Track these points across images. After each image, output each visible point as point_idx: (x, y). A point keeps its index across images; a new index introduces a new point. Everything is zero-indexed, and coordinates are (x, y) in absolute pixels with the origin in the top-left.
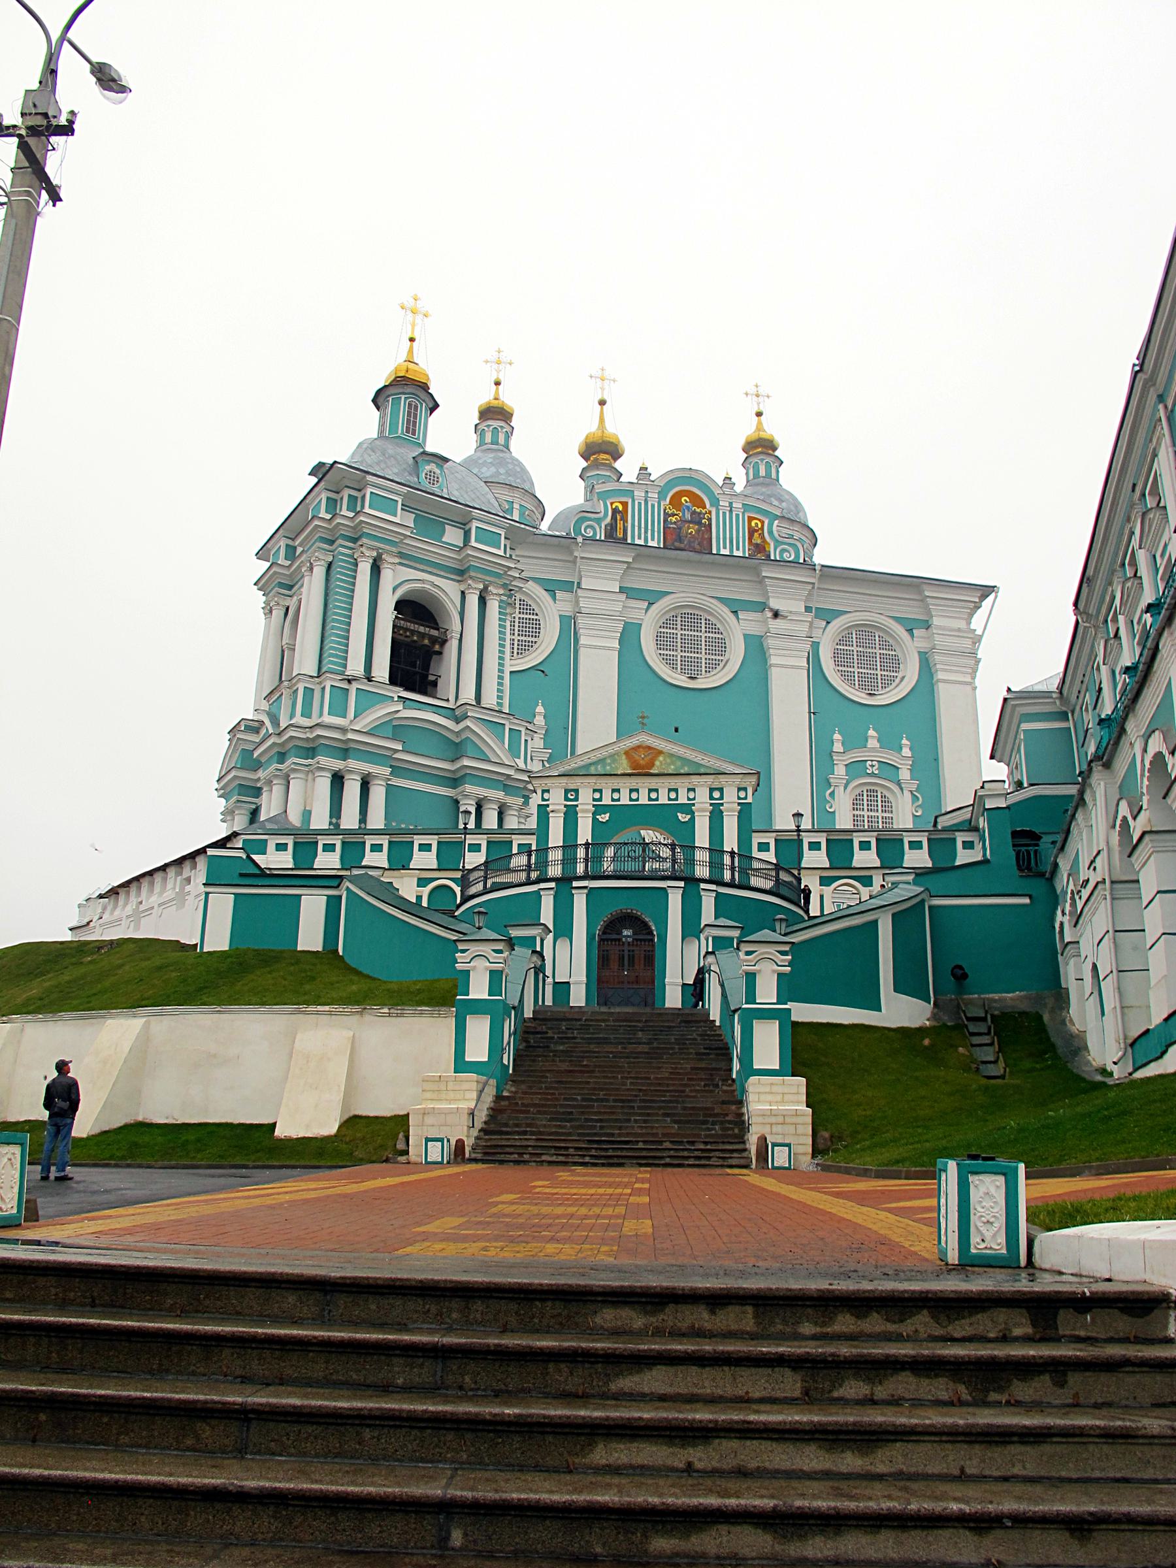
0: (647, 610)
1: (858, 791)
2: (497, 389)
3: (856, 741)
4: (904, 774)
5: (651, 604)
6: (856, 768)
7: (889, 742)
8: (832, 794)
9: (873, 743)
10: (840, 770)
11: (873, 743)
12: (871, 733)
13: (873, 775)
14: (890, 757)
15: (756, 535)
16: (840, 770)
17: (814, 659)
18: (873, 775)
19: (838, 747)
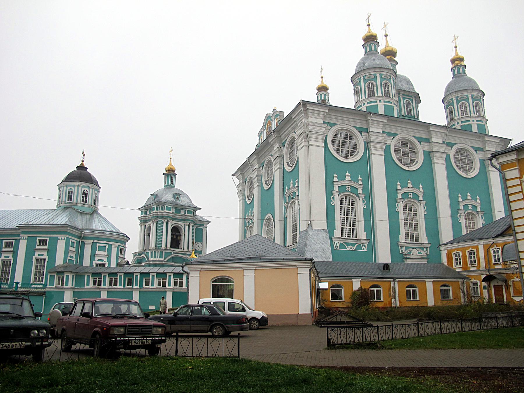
0: (263, 168)
2: (322, 80)
13: (292, 198)
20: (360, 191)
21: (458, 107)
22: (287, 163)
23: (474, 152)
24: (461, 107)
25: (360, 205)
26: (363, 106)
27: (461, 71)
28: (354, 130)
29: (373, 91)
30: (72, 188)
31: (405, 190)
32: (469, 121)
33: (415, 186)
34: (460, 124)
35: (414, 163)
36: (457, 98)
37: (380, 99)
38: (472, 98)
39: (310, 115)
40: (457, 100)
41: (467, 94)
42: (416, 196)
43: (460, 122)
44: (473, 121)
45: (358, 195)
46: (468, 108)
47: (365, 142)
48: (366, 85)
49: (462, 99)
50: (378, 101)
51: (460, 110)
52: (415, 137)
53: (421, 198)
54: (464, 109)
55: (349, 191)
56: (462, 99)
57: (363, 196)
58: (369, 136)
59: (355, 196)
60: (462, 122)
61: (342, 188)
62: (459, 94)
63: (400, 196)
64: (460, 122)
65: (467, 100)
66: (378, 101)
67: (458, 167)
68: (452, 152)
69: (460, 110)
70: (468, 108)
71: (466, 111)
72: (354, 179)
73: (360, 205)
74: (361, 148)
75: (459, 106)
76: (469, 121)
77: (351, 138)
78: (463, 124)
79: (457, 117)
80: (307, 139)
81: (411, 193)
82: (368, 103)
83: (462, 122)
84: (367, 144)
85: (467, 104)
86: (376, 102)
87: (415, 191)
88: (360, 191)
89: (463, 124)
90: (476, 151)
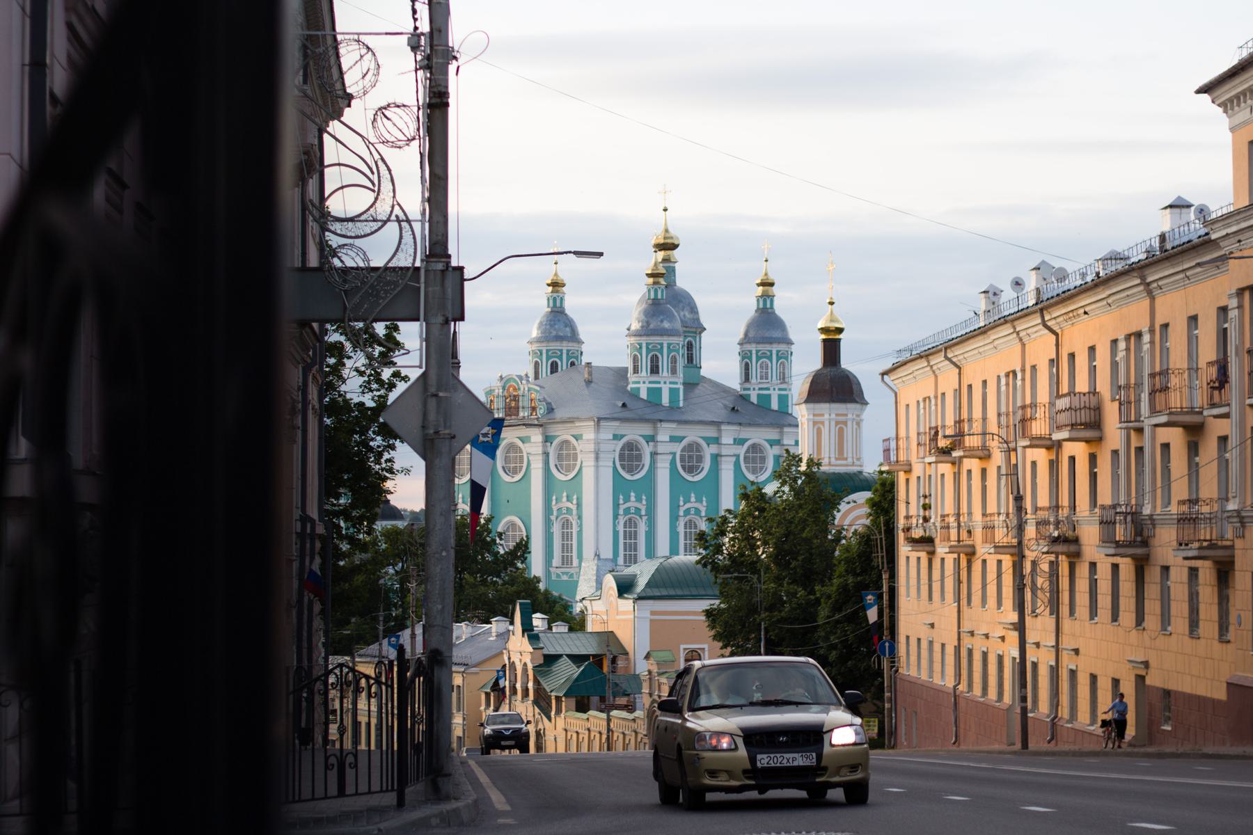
4: (575, 512)
7: (569, 499)
11: (564, 499)
14: (569, 505)
17: (546, 463)
19: (554, 503)
20: (643, 512)
22: (556, 465)
23: (768, 447)
25: (642, 528)
27: (768, 306)
29: (657, 367)
31: (688, 505)
33: (699, 500)
34: (757, 392)
36: (757, 352)
37: (665, 379)
38: (777, 355)
39: (601, 430)
40: (757, 355)
41: (770, 349)
42: (698, 511)
44: (774, 389)
45: (641, 516)
46: (770, 371)
47: (651, 453)
48: (649, 357)
49: (764, 355)
50: (662, 382)
51: (759, 370)
52: (703, 438)
56: (764, 355)
57: (646, 517)
58: (655, 446)
59: (638, 517)
60: (760, 389)
62: (760, 347)
63: (681, 513)
65: (770, 358)
66: (662, 382)
67: (747, 468)
68: (742, 451)
69: (759, 370)
70: (770, 371)
71: (767, 373)
72: (639, 500)
73: (642, 528)
74: (647, 460)
76: (768, 389)
77: (638, 449)
78: (761, 392)
79: (753, 381)
80: (597, 459)
82: (650, 382)
83: (760, 389)
84: (654, 454)
85: (770, 365)
86: (659, 383)
87: (697, 505)
88: (643, 512)
89: (761, 392)
90: (771, 446)
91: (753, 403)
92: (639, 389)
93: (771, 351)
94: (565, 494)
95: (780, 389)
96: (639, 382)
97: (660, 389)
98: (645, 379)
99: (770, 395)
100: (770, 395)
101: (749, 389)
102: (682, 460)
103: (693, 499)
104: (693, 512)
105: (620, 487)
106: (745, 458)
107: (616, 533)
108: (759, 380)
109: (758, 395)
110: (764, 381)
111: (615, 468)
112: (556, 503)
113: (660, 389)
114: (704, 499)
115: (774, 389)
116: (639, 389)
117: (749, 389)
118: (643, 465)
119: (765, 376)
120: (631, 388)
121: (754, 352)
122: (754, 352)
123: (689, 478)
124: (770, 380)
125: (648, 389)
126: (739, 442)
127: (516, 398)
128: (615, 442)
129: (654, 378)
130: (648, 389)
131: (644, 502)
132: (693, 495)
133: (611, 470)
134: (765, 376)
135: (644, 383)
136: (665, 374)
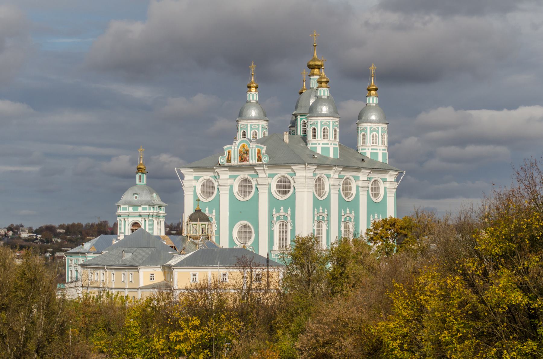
0: (234, 181)
1: (280, 223)
3: (278, 211)
4: (289, 218)
5: (235, 179)
6: (278, 218)
7: (286, 211)
8: (273, 226)
9: (282, 211)
10: (275, 219)
12: (282, 208)
13: (282, 219)
15: (259, 154)
16: (275, 219)
18: (282, 219)
19: (274, 213)
20: (326, 219)
21: (370, 136)
22: (275, 191)
24: (373, 136)
26: (317, 145)
28: (325, 176)
29: (327, 135)
30: (204, 226)
32: (377, 149)
33: (351, 213)
34: (370, 151)
35: (350, 195)
36: (371, 128)
40: (370, 130)
43: (370, 149)
50: (330, 144)
53: (352, 220)
54: (374, 139)
55: (321, 220)
61: (318, 217)
64: (370, 149)
65: (378, 132)
69: (371, 139)
70: (377, 139)
71: (376, 141)
72: (324, 212)
75: (371, 135)
76: (377, 149)
79: (368, 144)
81: (348, 217)
82: (323, 144)
83: (372, 149)
88: (326, 219)
91: (368, 158)
92: (316, 147)
93: (378, 128)
94: (282, 208)
95: (383, 150)
96: (316, 144)
97: (329, 148)
98: (319, 142)
99: (377, 153)
100: (377, 153)
101: (365, 149)
102: (343, 189)
103: (348, 212)
104: (348, 219)
105: (317, 204)
106: (372, 188)
107: (314, 230)
108: (371, 144)
109: (371, 153)
110: (374, 145)
111: (313, 193)
112: (276, 212)
113: (329, 148)
114: (353, 212)
115: (380, 150)
116: (316, 147)
117: (365, 149)
118: (326, 191)
119: (374, 142)
120: (311, 147)
121: (368, 128)
122: (368, 128)
123: (347, 200)
124: (377, 144)
125: (322, 147)
126: (369, 180)
127: (247, 152)
128: (314, 178)
129: (325, 141)
130: (322, 147)
131: (326, 213)
132: (348, 209)
133: (312, 193)
134: (374, 142)
135: (319, 144)
136: (331, 139)
